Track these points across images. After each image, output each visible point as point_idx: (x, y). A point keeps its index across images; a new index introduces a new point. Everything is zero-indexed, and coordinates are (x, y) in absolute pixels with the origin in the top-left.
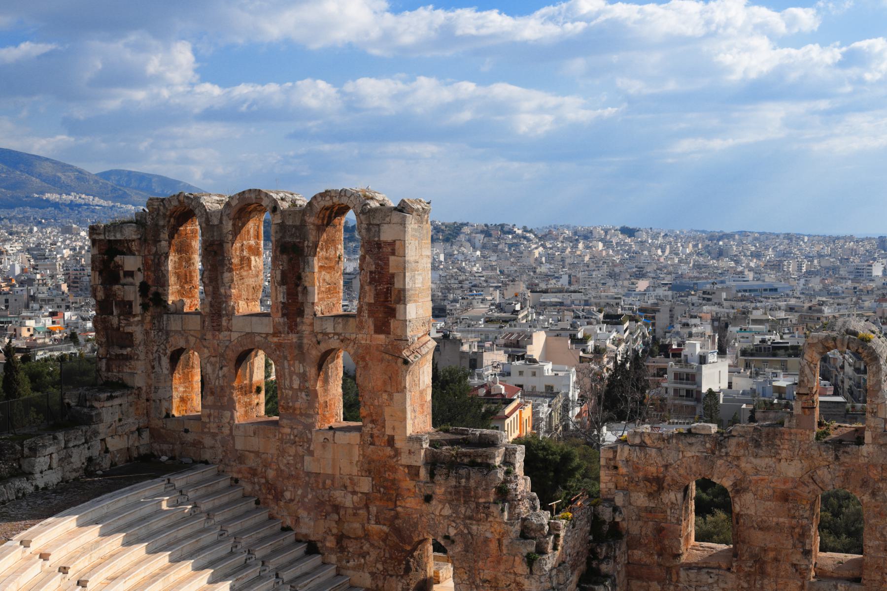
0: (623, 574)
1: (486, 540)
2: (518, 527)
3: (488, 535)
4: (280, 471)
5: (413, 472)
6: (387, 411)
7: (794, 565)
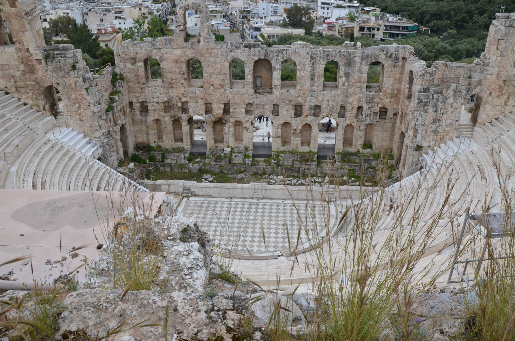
0: (126, 92)
1: (71, 84)
2: (81, 78)
3: (71, 82)
7: (182, 84)
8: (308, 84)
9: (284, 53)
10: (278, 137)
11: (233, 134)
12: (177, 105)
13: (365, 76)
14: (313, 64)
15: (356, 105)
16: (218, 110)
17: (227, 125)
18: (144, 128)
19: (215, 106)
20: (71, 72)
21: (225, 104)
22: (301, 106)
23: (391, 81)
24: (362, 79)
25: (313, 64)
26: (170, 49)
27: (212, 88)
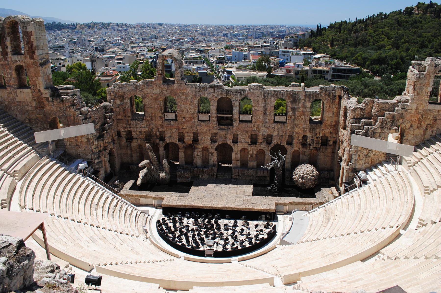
0: (115, 123)
1: (71, 116)
2: (79, 112)
4: (9, 102)
5: (47, 99)
6: (37, 82)
7: (160, 117)
8: (261, 118)
9: (242, 92)
10: (238, 160)
11: (200, 157)
12: (156, 133)
13: (308, 110)
14: (265, 101)
15: (301, 133)
16: (189, 138)
18: (129, 152)
19: (186, 135)
20: (71, 108)
21: (194, 133)
22: (256, 135)
23: (330, 114)
24: (306, 113)
25: (265, 101)
27: (184, 120)
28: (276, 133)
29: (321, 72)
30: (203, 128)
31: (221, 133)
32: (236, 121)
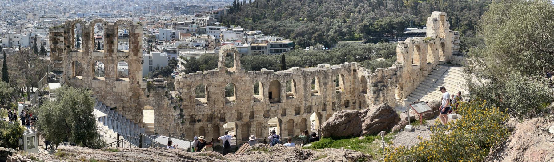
14: (305, 80)
17: (252, 127)
19: (244, 114)
22: (299, 108)
26: (216, 79)
28: (314, 104)
29: (259, 48)
30: (258, 108)
31: (272, 109)
32: (283, 98)
